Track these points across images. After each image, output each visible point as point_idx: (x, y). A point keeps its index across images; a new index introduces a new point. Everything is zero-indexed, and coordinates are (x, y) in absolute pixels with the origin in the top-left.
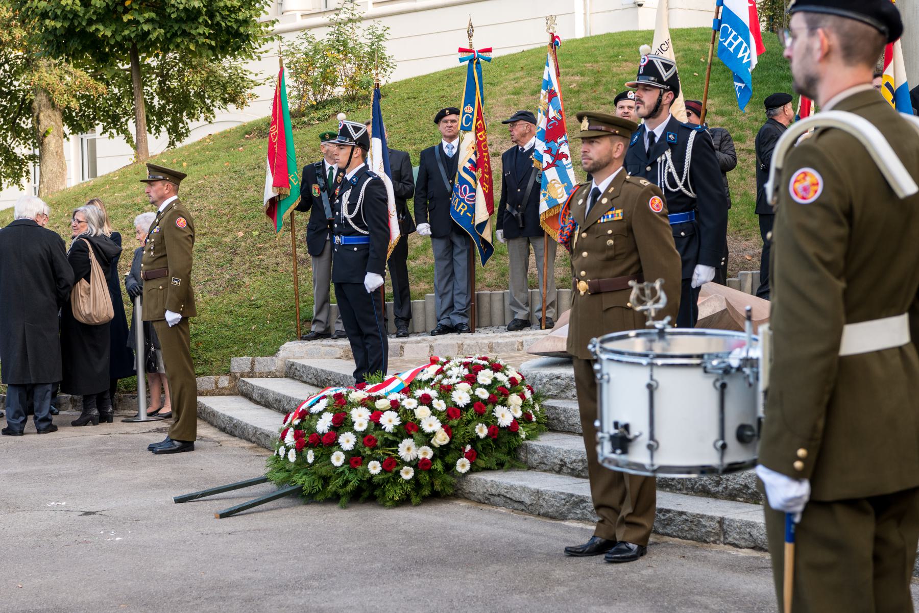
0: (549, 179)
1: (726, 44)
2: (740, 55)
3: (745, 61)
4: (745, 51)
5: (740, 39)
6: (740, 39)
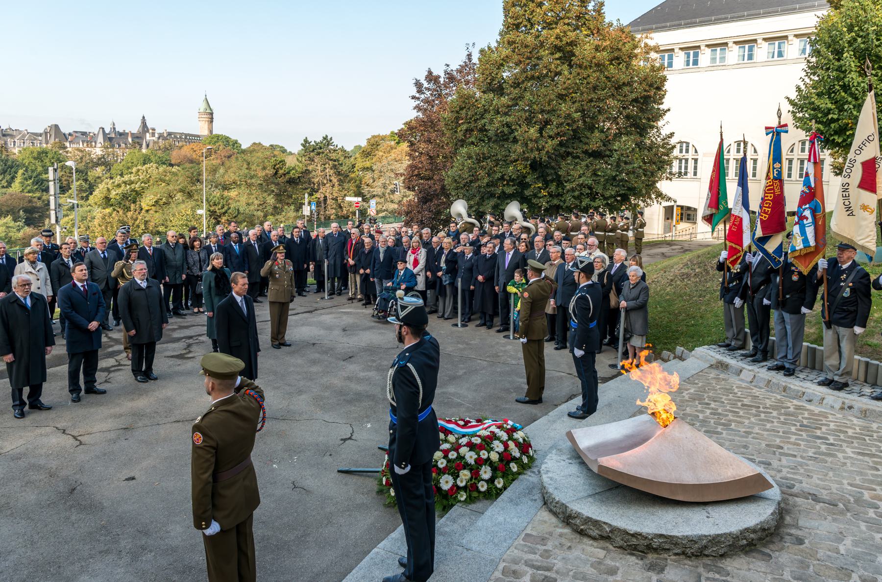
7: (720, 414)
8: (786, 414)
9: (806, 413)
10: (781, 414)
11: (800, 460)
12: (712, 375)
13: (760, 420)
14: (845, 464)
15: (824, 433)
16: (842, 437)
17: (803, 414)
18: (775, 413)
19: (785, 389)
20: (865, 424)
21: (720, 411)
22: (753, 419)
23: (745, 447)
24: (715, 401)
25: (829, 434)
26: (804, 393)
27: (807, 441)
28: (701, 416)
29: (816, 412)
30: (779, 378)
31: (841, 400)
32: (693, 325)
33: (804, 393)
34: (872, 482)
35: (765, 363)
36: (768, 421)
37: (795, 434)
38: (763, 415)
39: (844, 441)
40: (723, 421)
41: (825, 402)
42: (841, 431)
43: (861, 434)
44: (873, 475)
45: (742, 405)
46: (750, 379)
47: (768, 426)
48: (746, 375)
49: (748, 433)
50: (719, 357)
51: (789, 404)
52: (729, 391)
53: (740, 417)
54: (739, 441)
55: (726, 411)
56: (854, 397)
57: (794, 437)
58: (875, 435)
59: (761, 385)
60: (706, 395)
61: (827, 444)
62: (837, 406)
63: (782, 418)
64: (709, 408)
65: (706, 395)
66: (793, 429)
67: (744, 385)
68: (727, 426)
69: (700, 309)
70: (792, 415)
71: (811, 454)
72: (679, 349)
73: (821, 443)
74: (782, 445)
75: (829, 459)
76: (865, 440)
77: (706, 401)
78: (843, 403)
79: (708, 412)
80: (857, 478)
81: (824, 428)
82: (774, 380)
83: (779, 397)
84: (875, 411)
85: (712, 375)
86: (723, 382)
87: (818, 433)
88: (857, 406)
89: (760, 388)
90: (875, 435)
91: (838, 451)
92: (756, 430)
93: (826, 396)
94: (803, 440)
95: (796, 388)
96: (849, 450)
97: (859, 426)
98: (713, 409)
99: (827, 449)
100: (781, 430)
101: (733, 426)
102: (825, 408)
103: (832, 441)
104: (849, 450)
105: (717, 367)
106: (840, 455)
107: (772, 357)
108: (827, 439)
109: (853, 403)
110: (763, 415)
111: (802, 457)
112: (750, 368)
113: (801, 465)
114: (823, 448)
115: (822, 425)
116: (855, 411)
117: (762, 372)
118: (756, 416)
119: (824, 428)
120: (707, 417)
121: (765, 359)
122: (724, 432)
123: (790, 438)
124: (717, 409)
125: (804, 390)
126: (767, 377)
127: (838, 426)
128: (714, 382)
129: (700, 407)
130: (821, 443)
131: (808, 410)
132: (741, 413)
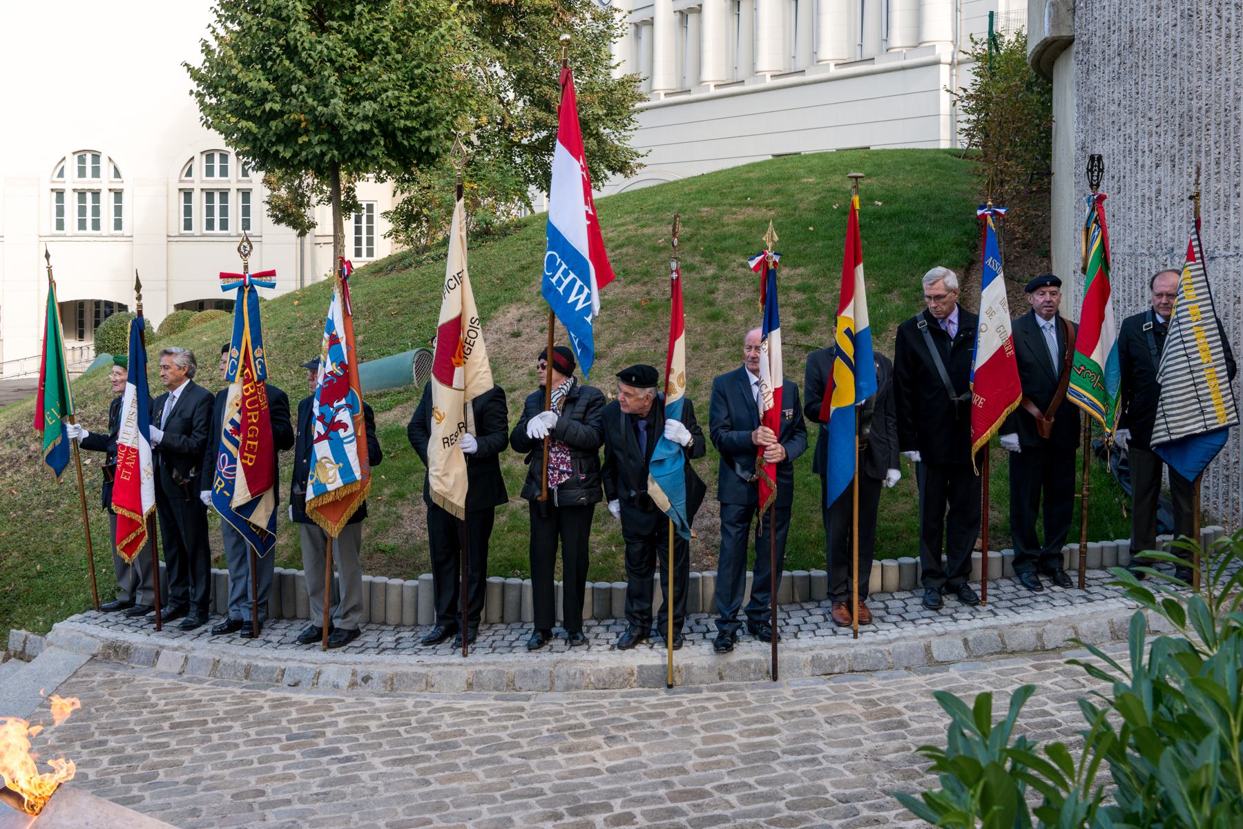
0: (319, 457)
1: (554, 280)
2: (571, 299)
3: (580, 306)
4: (581, 291)
5: (572, 276)
6: (572, 276)
7: (130, 758)
8: (259, 722)
9: (293, 709)
10: (248, 725)
11: (299, 806)
12: (98, 678)
13: (213, 748)
14: (375, 789)
15: (331, 741)
16: (362, 741)
17: (288, 714)
18: (237, 727)
19: (248, 672)
20: (394, 705)
21: (129, 751)
22: (198, 751)
23: (194, 812)
24: (116, 733)
25: (339, 741)
26: (283, 671)
27: (305, 765)
28: (92, 774)
29: (311, 704)
30: (238, 651)
31: (349, 669)
32: (40, 575)
33: (283, 671)
34: (423, 808)
35: (203, 628)
36: (228, 746)
37: (283, 758)
38: (215, 736)
39: (366, 746)
40: (139, 771)
41: (322, 679)
42: (359, 729)
43: (391, 724)
44: (422, 796)
45: (173, 726)
46: (177, 669)
47: (230, 755)
48: (169, 661)
49: (193, 782)
50: (109, 634)
51: (260, 701)
52: (141, 702)
53: (172, 752)
54: (180, 804)
55: (142, 747)
56: (371, 656)
57: (281, 764)
58: (413, 719)
59: (202, 674)
60: (94, 725)
61: (340, 761)
62: (344, 682)
63: (252, 732)
64: (105, 752)
65: (94, 725)
66: (276, 749)
67: (167, 683)
68: (148, 779)
69: (50, 534)
70: (270, 722)
71: (315, 790)
72: (17, 636)
73: (328, 763)
74: (261, 787)
75: (348, 789)
76: (399, 734)
77: (97, 737)
78: (354, 674)
79: (105, 759)
80: (399, 810)
81: (329, 731)
82: (225, 659)
83: (238, 691)
84: (406, 674)
85: (98, 678)
86: (124, 688)
87: (321, 743)
88: (376, 671)
89: (201, 681)
90: (413, 719)
91: (360, 768)
92: (209, 771)
93: (324, 668)
94: (297, 766)
95: (269, 664)
96: (376, 761)
97: (385, 710)
98: (113, 751)
99: (341, 770)
100: (254, 757)
101: (162, 777)
102: (324, 693)
103: (346, 753)
104: (376, 761)
105: (107, 658)
106: (365, 775)
107: (215, 612)
108: (338, 751)
109: (372, 668)
110: (215, 736)
111: (302, 800)
112: (175, 643)
113: (302, 815)
114: (334, 768)
115: (324, 726)
116: (375, 683)
117: (203, 647)
118: (203, 742)
119: (329, 731)
120: (105, 772)
121: (204, 619)
122: (147, 794)
123: (272, 769)
124: (122, 749)
125: (282, 665)
126: (211, 656)
127: (351, 720)
128: (105, 692)
129: (85, 755)
130: (328, 763)
131: (295, 703)
132: (173, 744)
